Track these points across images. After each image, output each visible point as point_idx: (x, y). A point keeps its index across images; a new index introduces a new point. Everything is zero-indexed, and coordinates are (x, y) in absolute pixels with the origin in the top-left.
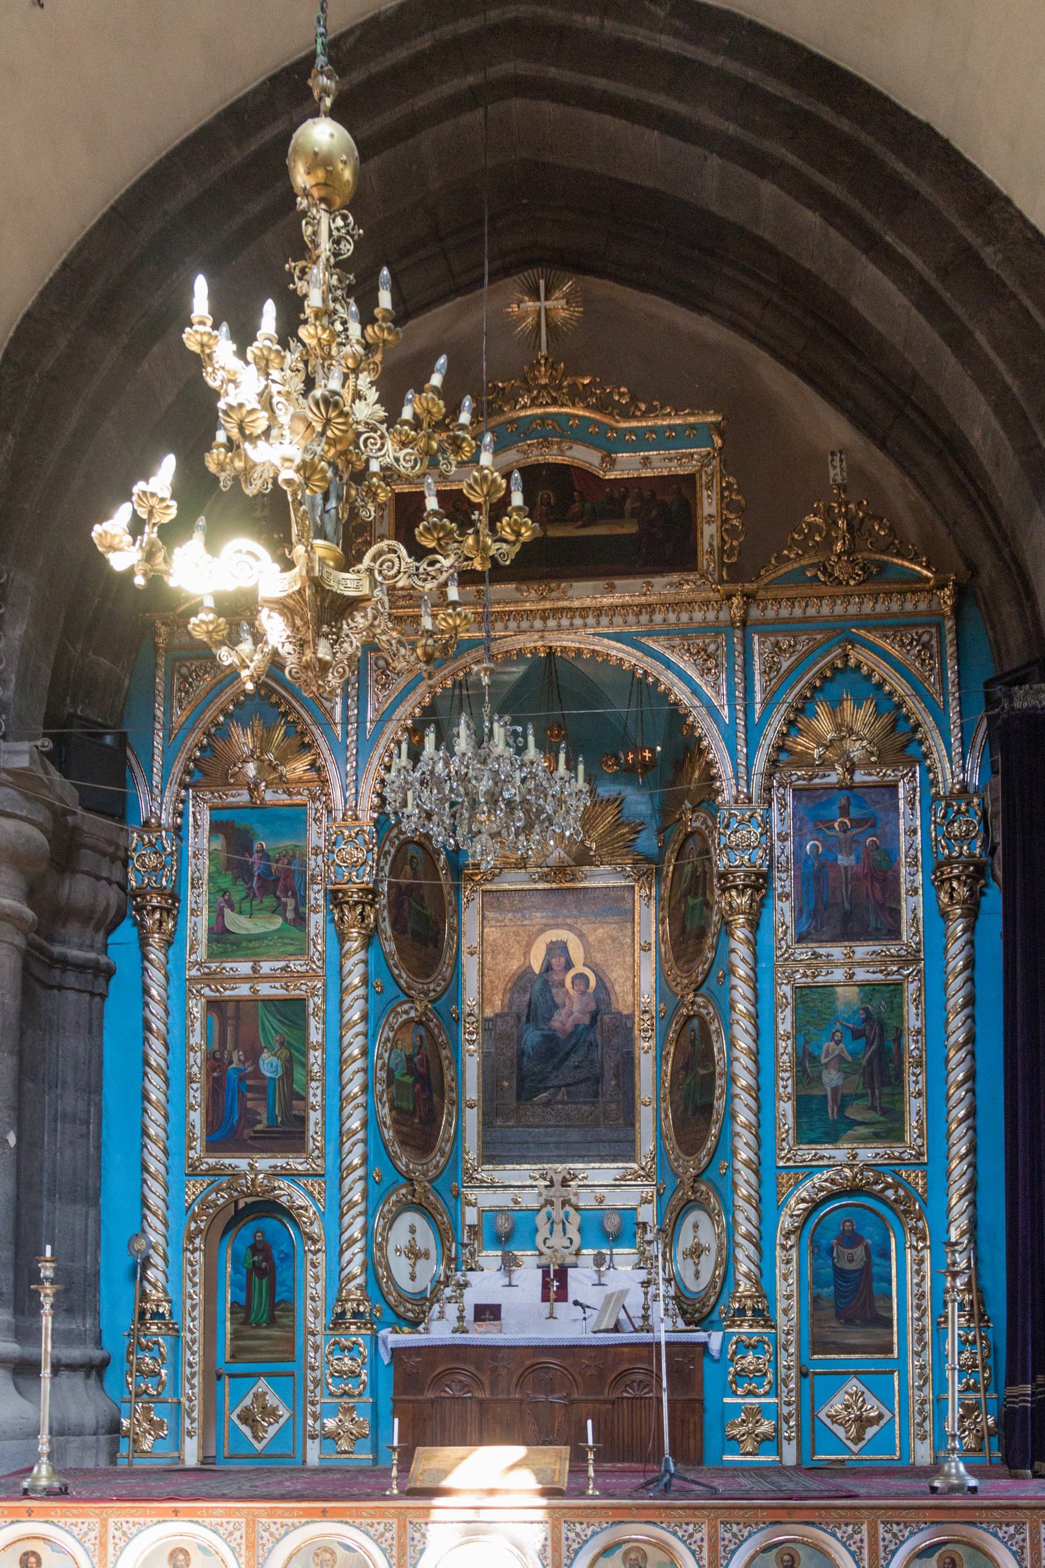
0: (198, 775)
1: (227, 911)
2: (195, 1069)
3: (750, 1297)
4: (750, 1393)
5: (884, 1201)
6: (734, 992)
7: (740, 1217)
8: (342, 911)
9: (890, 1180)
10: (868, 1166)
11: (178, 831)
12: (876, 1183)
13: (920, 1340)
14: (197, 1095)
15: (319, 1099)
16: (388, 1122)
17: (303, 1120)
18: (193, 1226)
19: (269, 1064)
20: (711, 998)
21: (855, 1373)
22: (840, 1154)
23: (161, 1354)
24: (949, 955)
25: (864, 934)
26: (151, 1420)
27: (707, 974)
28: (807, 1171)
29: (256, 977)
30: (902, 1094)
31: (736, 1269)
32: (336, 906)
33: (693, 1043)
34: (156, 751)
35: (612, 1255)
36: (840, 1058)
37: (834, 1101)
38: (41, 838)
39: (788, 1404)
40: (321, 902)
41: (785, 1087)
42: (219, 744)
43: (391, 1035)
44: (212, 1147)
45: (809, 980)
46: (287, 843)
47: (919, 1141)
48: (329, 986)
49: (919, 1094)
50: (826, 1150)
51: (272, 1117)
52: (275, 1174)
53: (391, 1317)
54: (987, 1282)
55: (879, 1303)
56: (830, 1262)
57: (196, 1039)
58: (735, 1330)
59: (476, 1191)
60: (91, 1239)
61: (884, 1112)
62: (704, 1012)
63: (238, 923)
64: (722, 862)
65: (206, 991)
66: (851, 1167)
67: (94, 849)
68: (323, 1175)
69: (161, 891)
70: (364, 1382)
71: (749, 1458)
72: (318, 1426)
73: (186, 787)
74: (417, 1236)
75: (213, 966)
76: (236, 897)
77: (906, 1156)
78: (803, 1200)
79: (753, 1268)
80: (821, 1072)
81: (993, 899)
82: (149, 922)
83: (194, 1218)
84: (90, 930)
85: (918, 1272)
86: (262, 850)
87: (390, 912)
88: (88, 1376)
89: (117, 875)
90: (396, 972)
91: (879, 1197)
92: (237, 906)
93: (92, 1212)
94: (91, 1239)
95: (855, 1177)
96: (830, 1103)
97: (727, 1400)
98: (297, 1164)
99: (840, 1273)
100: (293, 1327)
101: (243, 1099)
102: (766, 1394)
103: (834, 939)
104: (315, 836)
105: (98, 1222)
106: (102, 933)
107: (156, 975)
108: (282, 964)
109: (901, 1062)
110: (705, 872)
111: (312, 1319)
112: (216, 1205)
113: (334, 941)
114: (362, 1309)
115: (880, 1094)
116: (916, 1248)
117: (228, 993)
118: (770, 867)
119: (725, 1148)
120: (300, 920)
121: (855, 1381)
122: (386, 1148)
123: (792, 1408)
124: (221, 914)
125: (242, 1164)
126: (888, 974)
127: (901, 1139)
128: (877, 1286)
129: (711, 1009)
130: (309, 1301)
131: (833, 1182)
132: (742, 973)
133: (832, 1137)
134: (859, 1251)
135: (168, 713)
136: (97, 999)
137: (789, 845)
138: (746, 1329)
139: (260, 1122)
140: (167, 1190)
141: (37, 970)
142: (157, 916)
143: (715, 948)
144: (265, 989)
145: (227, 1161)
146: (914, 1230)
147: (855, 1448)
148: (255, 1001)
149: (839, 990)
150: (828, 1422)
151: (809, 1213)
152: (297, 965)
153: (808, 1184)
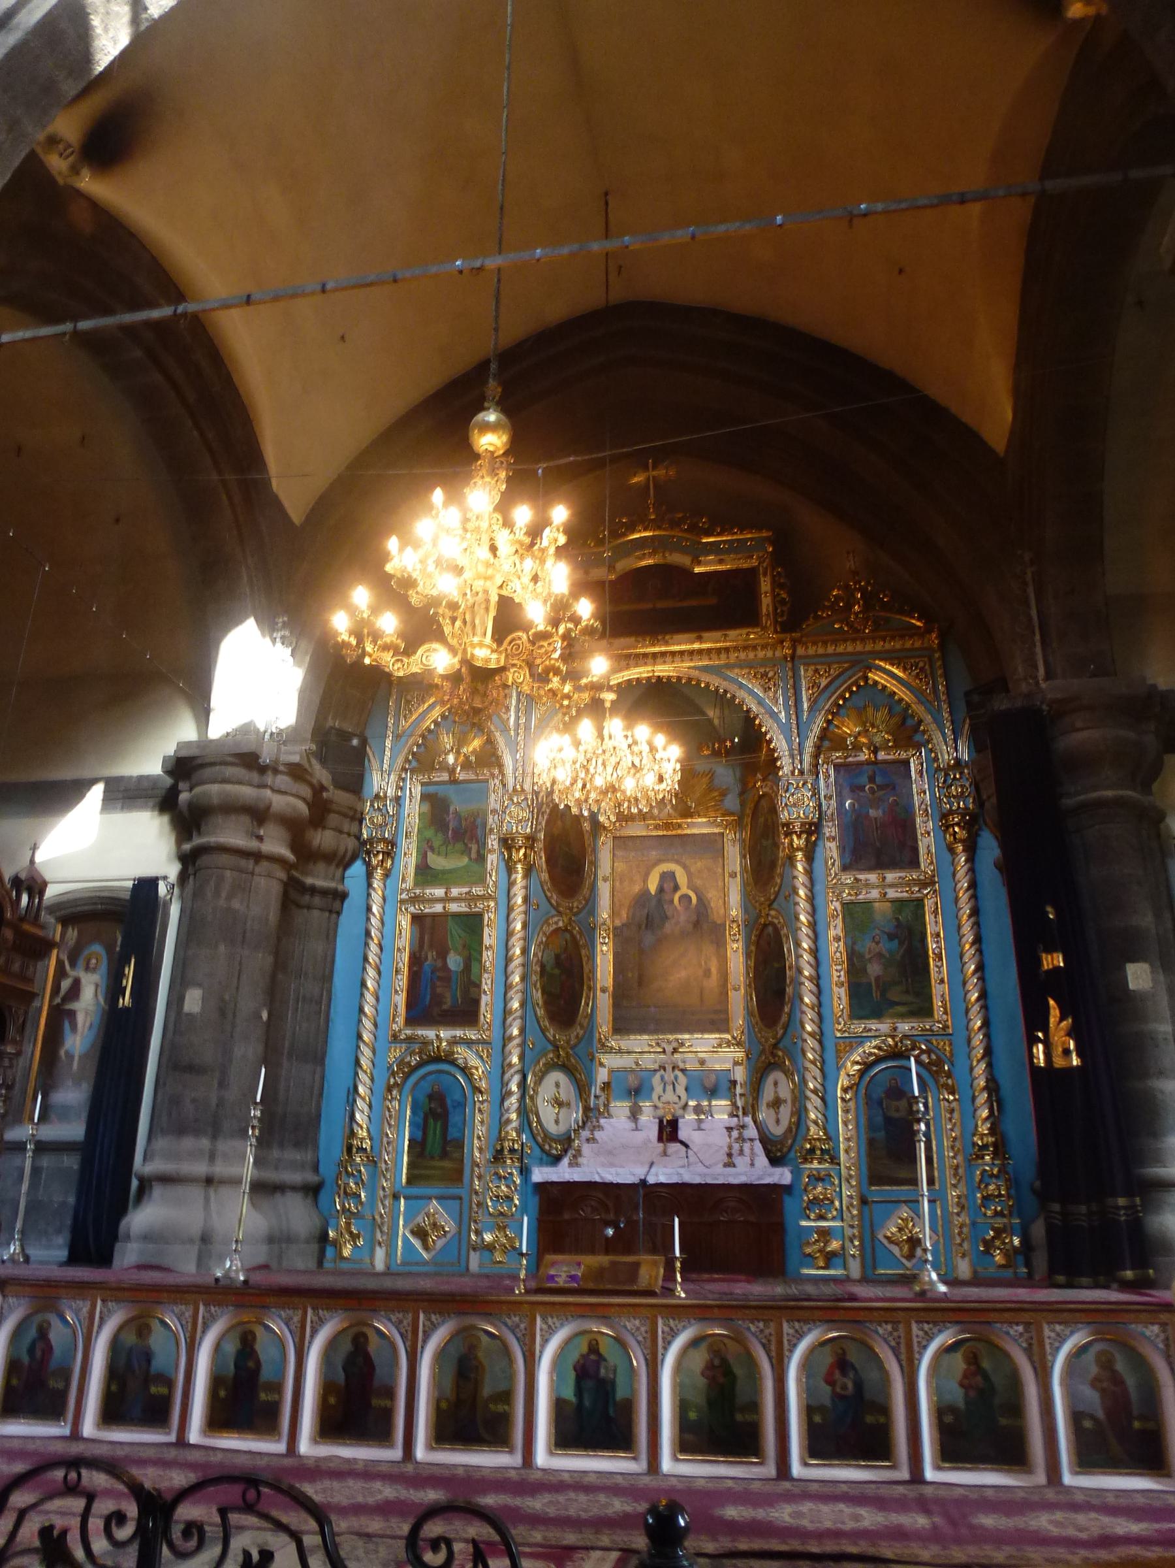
0: (414, 764)
1: (429, 854)
3: (818, 1139)
4: (821, 1217)
6: (797, 907)
7: (808, 1076)
9: (923, 1047)
10: (905, 1037)
11: (398, 800)
13: (956, 1175)
14: (402, 981)
15: (490, 986)
16: (540, 1002)
17: (477, 1002)
18: (392, 1081)
19: (454, 962)
21: (905, 1202)
22: (884, 1027)
23: (362, 1180)
25: (893, 865)
26: (351, 1233)
27: (777, 894)
28: (859, 1040)
29: (447, 899)
31: (807, 1117)
33: (769, 944)
34: (387, 749)
35: (710, 1105)
36: (880, 955)
37: (878, 986)
38: (303, 808)
39: (852, 1227)
40: (496, 847)
41: (839, 977)
43: (544, 939)
44: (411, 1021)
45: (853, 898)
47: (945, 1017)
50: (874, 1025)
52: (454, 1042)
53: (537, 1151)
54: (1010, 1128)
56: (881, 1112)
58: (808, 1166)
59: (607, 1056)
60: (316, 1092)
62: (776, 921)
64: (784, 816)
65: (412, 909)
66: (893, 1037)
67: (339, 813)
68: (490, 1043)
69: (384, 840)
70: (516, 1206)
72: (479, 1241)
73: (404, 770)
74: (561, 1091)
75: (418, 891)
76: (437, 843)
77: (935, 1028)
78: (857, 1063)
79: (820, 1116)
80: (866, 966)
81: (990, 848)
82: (374, 862)
83: (393, 1074)
84: (333, 867)
85: (950, 1119)
86: (456, 812)
88: (306, 1195)
89: (354, 829)
90: (549, 894)
92: (436, 850)
93: (319, 1069)
94: (316, 1092)
95: (896, 1044)
96: (874, 988)
97: (804, 1223)
98: (472, 1035)
99: (888, 1120)
100: (462, 1160)
101: (433, 988)
102: (834, 1218)
103: (870, 869)
104: (493, 802)
105: (323, 1078)
106: (341, 869)
107: (376, 897)
108: (467, 890)
109: (927, 956)
110: (773, 823)
111: (478, 1155)
112: (410, 1065)
114: (516, 1146)
116: (948, 1100)
117: (427, 911)
118: (820, 818)
119: (793, 1025)
120: (481, 859)
121: (906, 1208)
122: (538, 1022)
123: (856, 1231)
124: (425, 856)
125: (430, 1034)
126: (912, 893)
129: (782, 921)
130: (476, 1142)
131: (879, 1048)
134: (903, 1104)
136: (334, 916)
137: (833, 802)
138: (815, 1165)
139: (445, 1003)
140: (374, 1052)
141: (293, 894)
142: (380, 857)
143: (782, 876)
144: (454, 907)
145: (420, 1032)
146: (946, 1086)
147: (908, 1264)
148: (445, 915)
149: (877, 905)
150: (885, 1242)
151: (862, 1073)
152: (477, 890)
153: (861, 1050)
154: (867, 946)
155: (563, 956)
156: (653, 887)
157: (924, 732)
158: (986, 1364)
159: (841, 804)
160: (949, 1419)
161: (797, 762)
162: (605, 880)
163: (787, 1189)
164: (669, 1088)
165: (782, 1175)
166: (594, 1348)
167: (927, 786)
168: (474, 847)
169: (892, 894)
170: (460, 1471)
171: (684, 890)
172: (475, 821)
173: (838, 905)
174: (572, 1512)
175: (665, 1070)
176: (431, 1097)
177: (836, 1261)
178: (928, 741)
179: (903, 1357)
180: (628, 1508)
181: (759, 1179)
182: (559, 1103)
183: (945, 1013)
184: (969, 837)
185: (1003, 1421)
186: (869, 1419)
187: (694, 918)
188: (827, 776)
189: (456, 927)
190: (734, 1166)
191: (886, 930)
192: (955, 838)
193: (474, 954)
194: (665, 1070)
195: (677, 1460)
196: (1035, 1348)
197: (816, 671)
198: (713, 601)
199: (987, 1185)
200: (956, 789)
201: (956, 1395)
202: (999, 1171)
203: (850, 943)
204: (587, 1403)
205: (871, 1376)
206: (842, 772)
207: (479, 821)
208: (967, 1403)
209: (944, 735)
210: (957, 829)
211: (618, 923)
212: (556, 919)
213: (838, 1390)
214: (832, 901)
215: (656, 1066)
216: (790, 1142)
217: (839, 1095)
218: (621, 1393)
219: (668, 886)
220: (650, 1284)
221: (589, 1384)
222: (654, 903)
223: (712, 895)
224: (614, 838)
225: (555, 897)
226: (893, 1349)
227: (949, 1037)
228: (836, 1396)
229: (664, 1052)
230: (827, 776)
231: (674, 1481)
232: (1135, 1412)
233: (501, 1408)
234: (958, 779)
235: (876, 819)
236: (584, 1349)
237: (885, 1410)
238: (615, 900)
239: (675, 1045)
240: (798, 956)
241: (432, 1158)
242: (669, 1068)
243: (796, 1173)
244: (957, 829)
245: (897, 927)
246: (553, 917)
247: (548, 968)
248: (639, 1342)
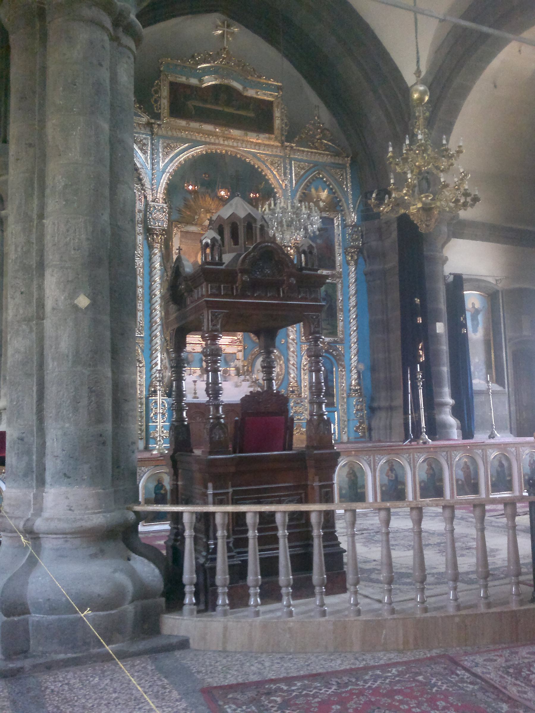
5: (333, 355)
24: (350, 276)
32: (150, 234)
49: (342, 321)
113: (146, 247)
157: (341, 206)
158: (433, 466)
179: (412, 465)
185: (438, 484)
186: (399, 487)
192: (352, 259)
199: (358, 405)
208: (428, 479)
213: (390, 478)
226: (408, 462)
228: (390, 480)
232: (472, 477)
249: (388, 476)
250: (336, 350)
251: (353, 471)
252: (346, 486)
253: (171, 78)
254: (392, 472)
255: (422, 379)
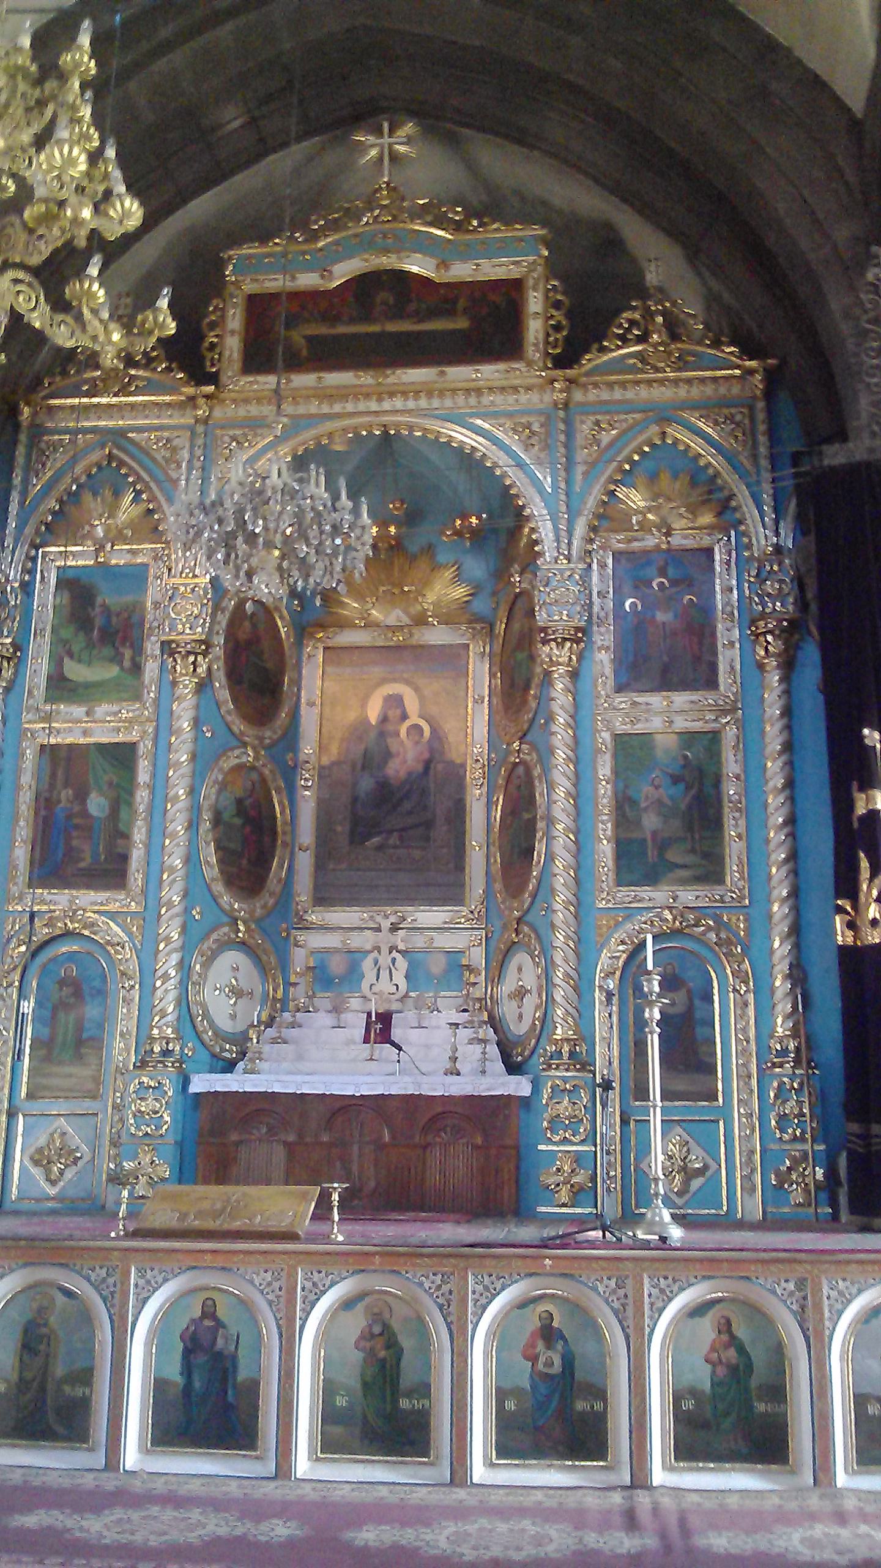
1: (66, 660)
2: (23, 807)
4: (565, 1141)
5: (706, 944)
8: (175, 660)
12: (696, 925)
17: (125, 858)
19: (97, 805)
20: (534, 747)
22: (659, 895)
27: (532, 721)
30: (723, 838)
36: (659, 802)
42: (70, 509)
43: (220, 777)
46: (129, 599)
47: (741, 884)
48: (161, 729)
50: (645, 892)
51: (95, 855)
55: (703, 1049)
57: (27, 779)
58: (553, 1073)
61: (706, 855)
63: (75, 671)
71: (564, 1210)
76: (76, 648)
86: (104, 605)
87: (225, 662)
90: (229, 718)
91: (699, 940)
92: (76, 656)
97: (540, 1147)
101: (68, 839)
102: (582, 1142)
113: (166, 686)
115: (701, 838)
120: (137, 669)
121: (679, 1130)
127: (721, 881)
128: (700, 1032)
132: (562, 720)
133: (651, 878)
135: (26, 481)
139: (83, 860)
154: (645, 791)
155: (248, 802)
156: (373, 715)
157: (735, 509)
158: (741, 1331)
159: (619, 604)
160: (688, 1405)
161: (564, 546)
162: (311, 704)
163: (525, 1103)
164: (384, 974)
165: (520, 1086)
166: (209, 1312)
167: (734, 582)
168: (128, 653)
169: (681, 724)
170: (17, 1477)
171: (414, 719)
172: (130, 617)
173: (606, 736)
174: (138, 1538)
175: (379, 952)
176: (62, 983)
177: (582, 1196)
178: (741, 522)
180: (223, 1531)
181: (489, 1090)
182: (237, 993)
183: (742, 878)
184: (786, 650)
185: (761, 1407)
186: (580, 1405)
187: (426, 755)
188: (603, 566)
189: (101, 760)
190: (458, 1074)
191: (670, 771)
193: (123, 794)
194: (379, 952)
195: (318, 1459)
196: (809, 1311)
197: (597, 423)
198: (462, 323)
200: (772, 586)
201: (702, 1377)
202: (801, 1084)
203: (621, 785)
204: (197, 1384)
205: (584, 1348)
206: (623, 561)
207: (135, 619)
209: (762, 515)
210: (769, 638)
211: (325, 761)
212: (237, 752)
214: (599, 732)
215: (368, 947)
216: (533, 1041)
217: (597, 983)
218: (243, 1375)
219: (395, 713)
220: (291, 1224)
221: (201, 1359)
222: (373, 735)
223: (450, 726)
224: (325, 648)
225: (237, 722)
227: (746, 910)
229: (378, 929)
230: (603, 566)
231: (307, 1488)
233: (79, 1392)
234: (776, 572)
235: (664, 623)
236: (197, 1313)
237: (601, 1395)
238: (323, 730)
239: (393, 919)
240: (551, 802)
241: (60, 1063)
242: (385, 950)
243: (536, 1085)
244: (769, 638)
245: (684, 767)
246: (232, 749)
247: (226, 816)
248: (270, 1303)
249: (534, 1359)
250: (720, 924)
251: (386, 1327)
252: (355, 1383)
253: (249, 287)
254: (549, 1346)
255: (659, 996)
